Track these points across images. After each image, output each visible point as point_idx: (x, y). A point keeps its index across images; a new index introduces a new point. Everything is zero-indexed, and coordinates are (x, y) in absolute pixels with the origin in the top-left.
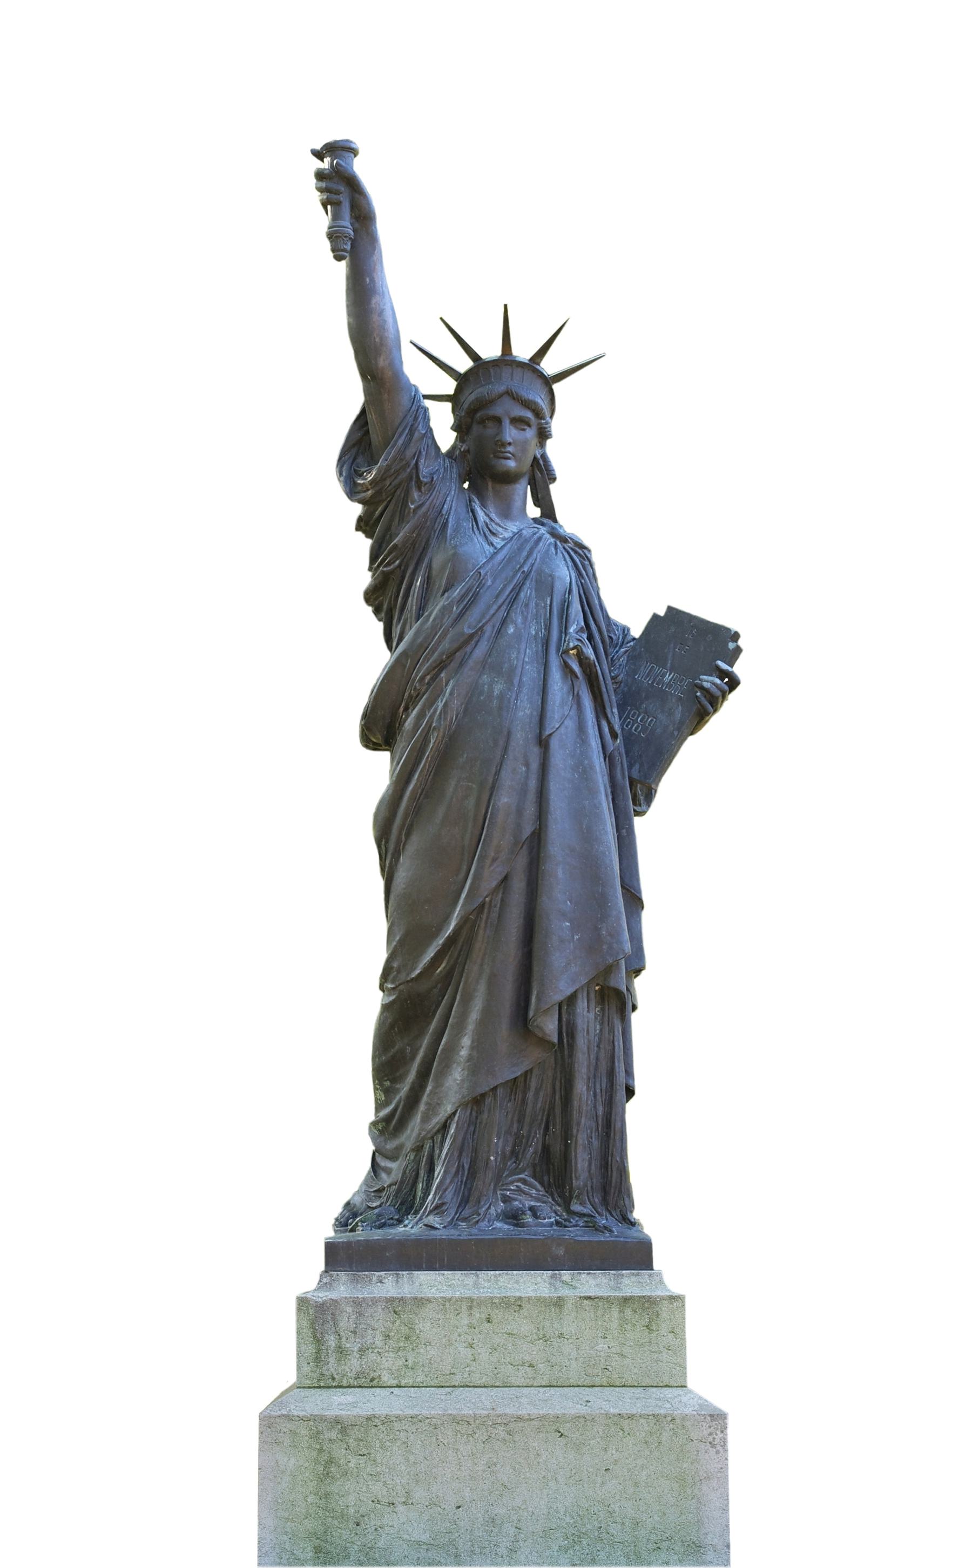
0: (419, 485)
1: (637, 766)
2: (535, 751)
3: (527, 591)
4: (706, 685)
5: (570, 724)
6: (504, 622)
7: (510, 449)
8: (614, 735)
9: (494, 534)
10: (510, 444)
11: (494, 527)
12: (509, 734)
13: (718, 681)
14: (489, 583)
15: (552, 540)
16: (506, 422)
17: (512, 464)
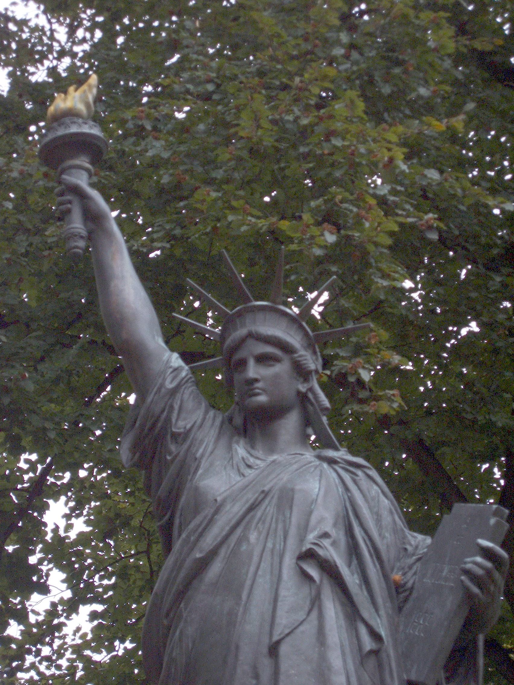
0: (175, 437)
1: (415, 667)
2: (266, 663)
3: (269, 508)
4: (469, 566)
5: (309, 628)
6: (239, 542)
7: (259, 385)
8: (375, 636)
9: (249, 467)
10: (256, 380)
11: (252, 460)
12: (237, 647)
13: (479, 559)
14: (228, 507)
15: (317, 462)
16: (251, 363)
17: (262, 399)
